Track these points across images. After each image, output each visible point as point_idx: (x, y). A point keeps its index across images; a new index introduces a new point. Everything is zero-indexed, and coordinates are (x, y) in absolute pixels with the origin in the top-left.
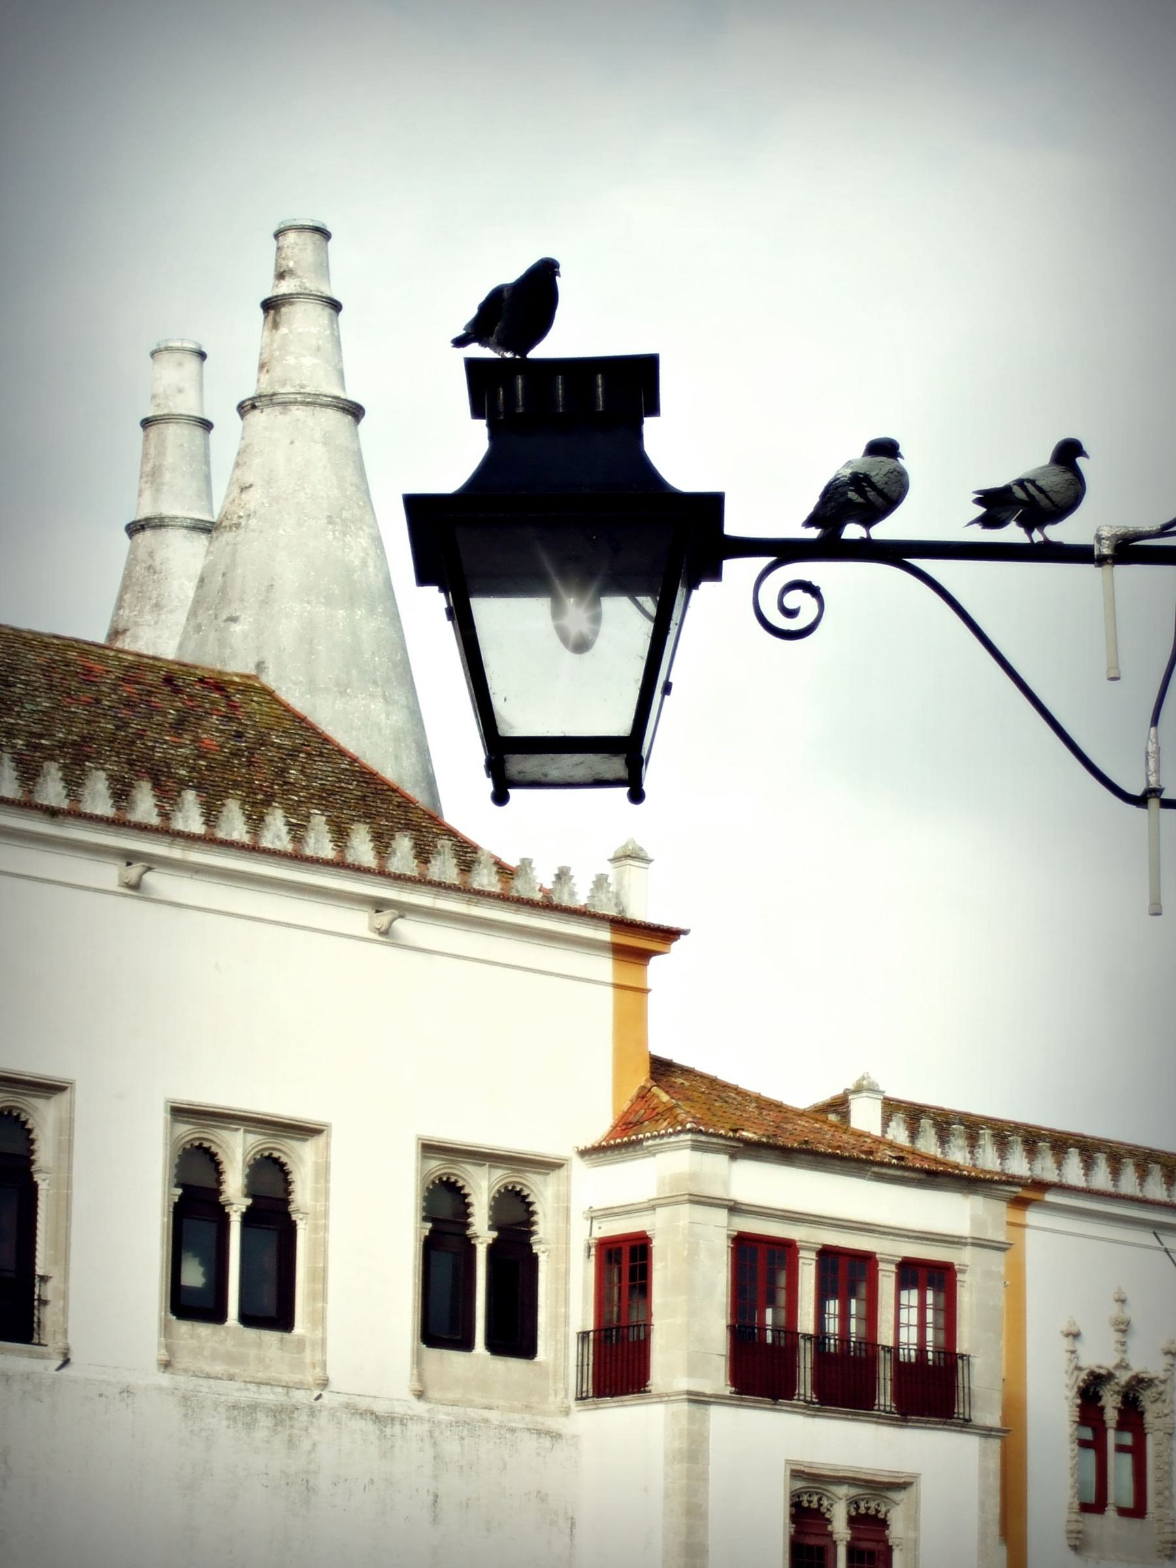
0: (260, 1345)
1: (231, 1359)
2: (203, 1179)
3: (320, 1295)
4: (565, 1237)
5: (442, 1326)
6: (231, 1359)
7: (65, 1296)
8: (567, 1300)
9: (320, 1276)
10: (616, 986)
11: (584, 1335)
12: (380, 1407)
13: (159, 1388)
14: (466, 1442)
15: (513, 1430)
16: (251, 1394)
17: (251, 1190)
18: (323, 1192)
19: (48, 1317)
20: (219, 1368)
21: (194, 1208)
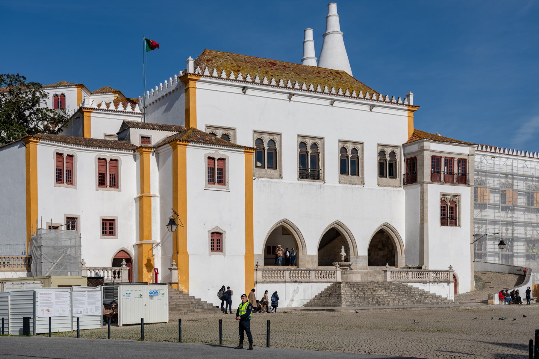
0: (354, 178)
5: (382, 173)
6: (349, 181)
7: (324, 172)
8: (402, 168)
9: (363, 167)
17: (352, 153)
18: (363, 154)
19: (321, 175)
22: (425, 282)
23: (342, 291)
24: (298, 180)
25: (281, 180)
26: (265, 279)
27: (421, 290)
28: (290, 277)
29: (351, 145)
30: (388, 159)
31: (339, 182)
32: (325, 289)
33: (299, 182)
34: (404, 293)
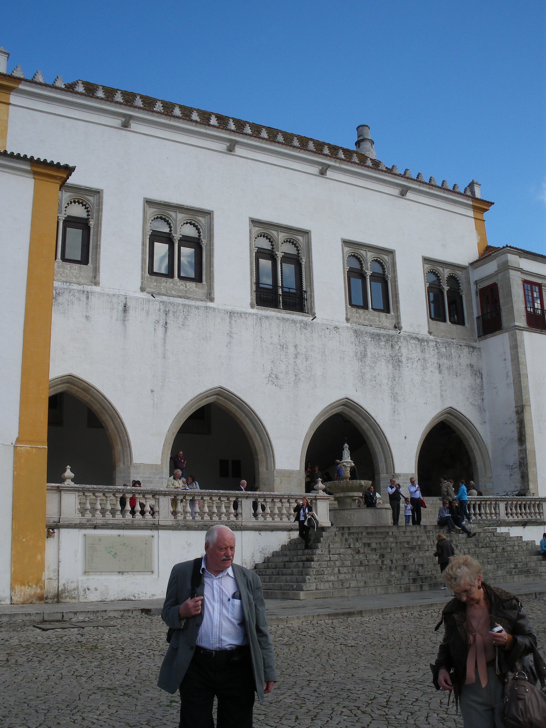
1: (369, 320)
2: (357, 266)
3: (397, 302)
4: (470, 289)
5: (437, 313)
6: (369, 320)
7: (312, 297)
8: (472, 308)
9: (396, 295)
10: (475, 218)
11: (478, 318)
12: (420, 337)
13: (348, 328)
14: (447, 348)
15: (461, 346)
16: (377, 331)
18: (394, 271)
19: (307, 304)
20: (366, 323)
21: (355, 274)
22: (524, 524)
23: (318, 552)
24: (252, 307)
25: (210, 304)
26: (88, 516)
27: (527, 543)
28: (174, 513)
29: (369, 254)
30: (446, 288)
31: (347, 320)
32: (284, 547)
33: (254, 311)
34: (488, 550)
